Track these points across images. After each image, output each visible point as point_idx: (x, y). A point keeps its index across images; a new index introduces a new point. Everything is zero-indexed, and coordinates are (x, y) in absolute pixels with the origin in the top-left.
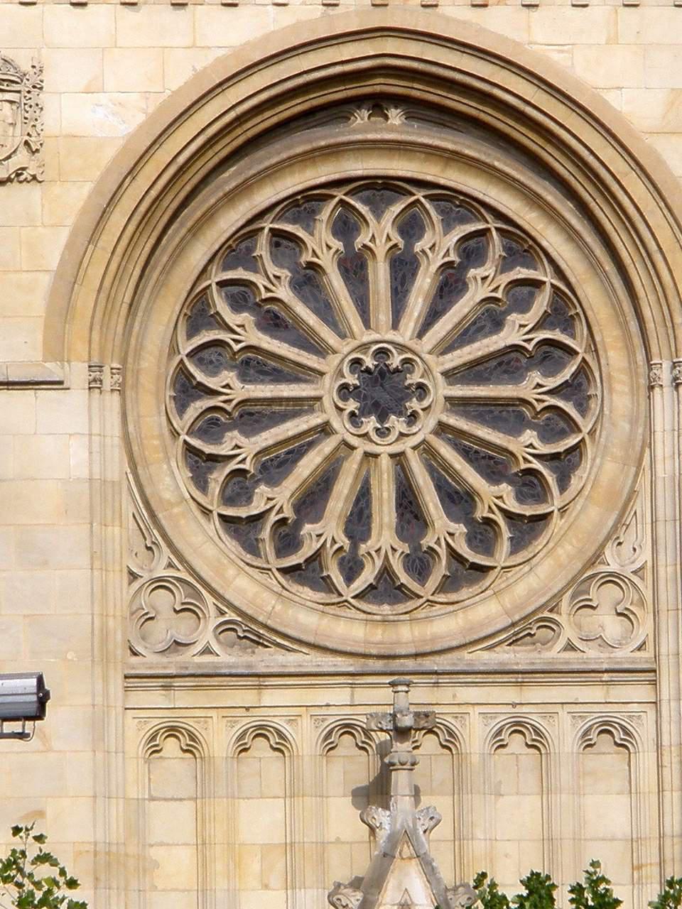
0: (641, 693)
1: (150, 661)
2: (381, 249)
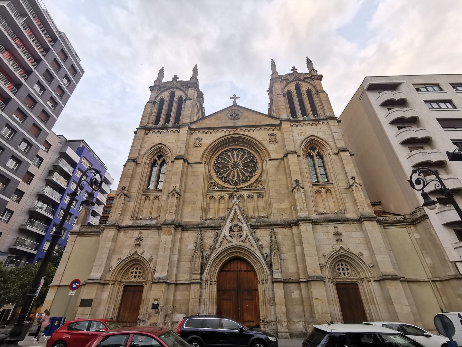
0: (263, 191)
1: (210, 189)
2: (235, 154)
